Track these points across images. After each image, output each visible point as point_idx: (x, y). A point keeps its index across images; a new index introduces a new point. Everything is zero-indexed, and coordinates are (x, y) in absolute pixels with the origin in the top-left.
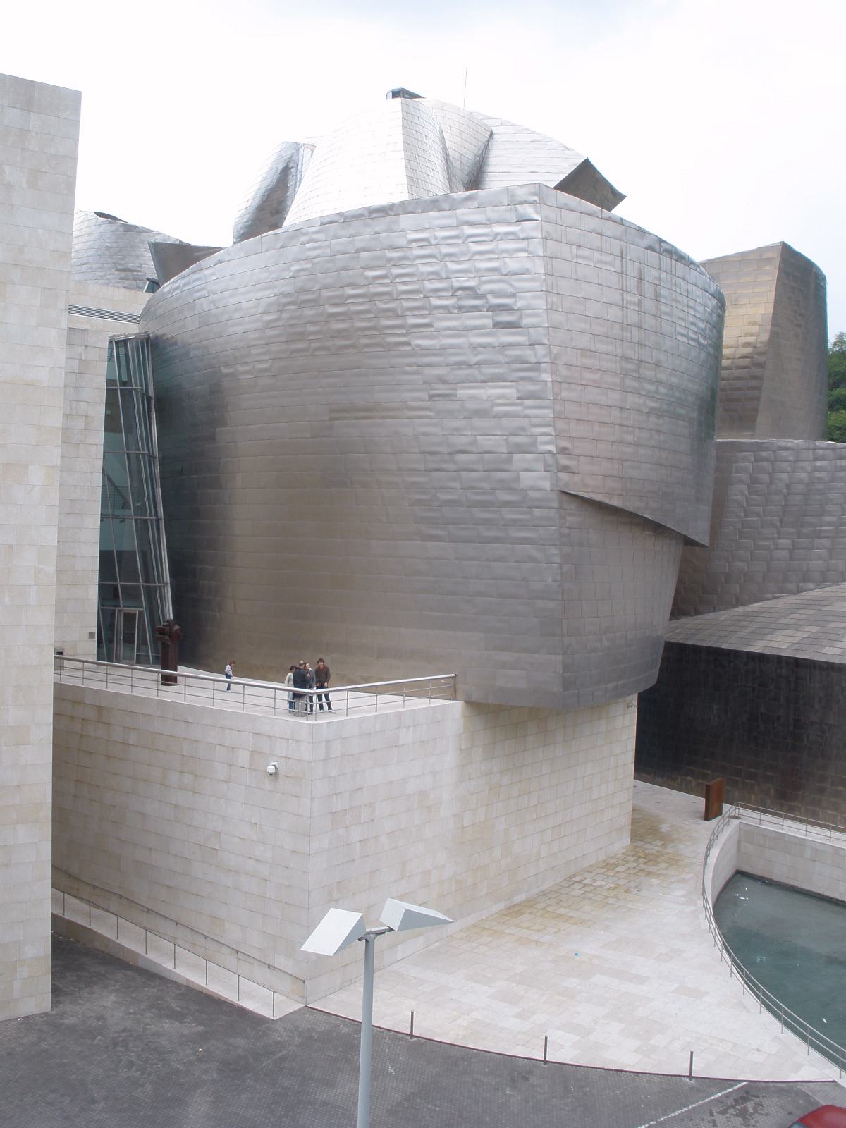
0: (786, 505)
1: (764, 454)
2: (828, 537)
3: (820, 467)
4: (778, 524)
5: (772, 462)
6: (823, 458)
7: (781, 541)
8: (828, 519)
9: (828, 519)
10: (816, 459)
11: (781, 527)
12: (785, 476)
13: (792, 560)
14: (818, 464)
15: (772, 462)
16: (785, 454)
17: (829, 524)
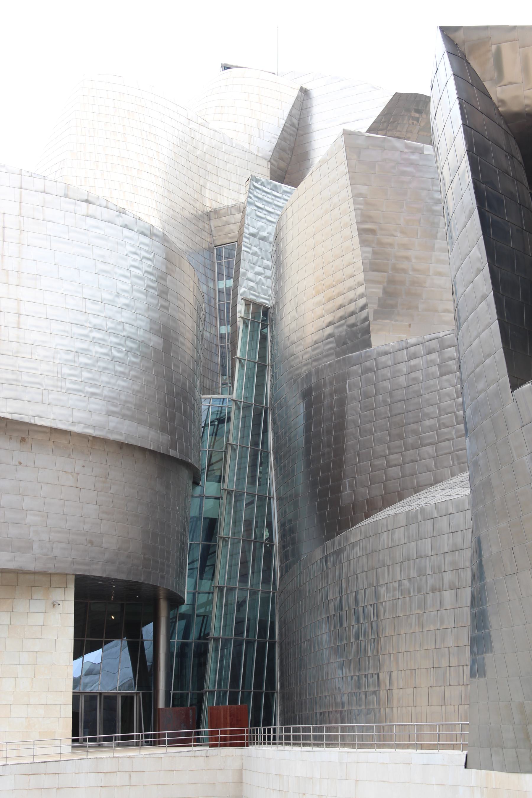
0: (392, 416)
1: (368, 364)
2: (431, 444)
3: (415, 366)
4: (388, 438)
5: (375, 371)
6: (414, 356)
7: (392, 457)
8: (427, 423)
9: (427, 423)
10: (410, 359)
11: (391, 441)
12: (387, 384)
13: (403, 477)
14: (413, 362)
15: (375, 371)
16: (383, 359)
17: (431, 428)
